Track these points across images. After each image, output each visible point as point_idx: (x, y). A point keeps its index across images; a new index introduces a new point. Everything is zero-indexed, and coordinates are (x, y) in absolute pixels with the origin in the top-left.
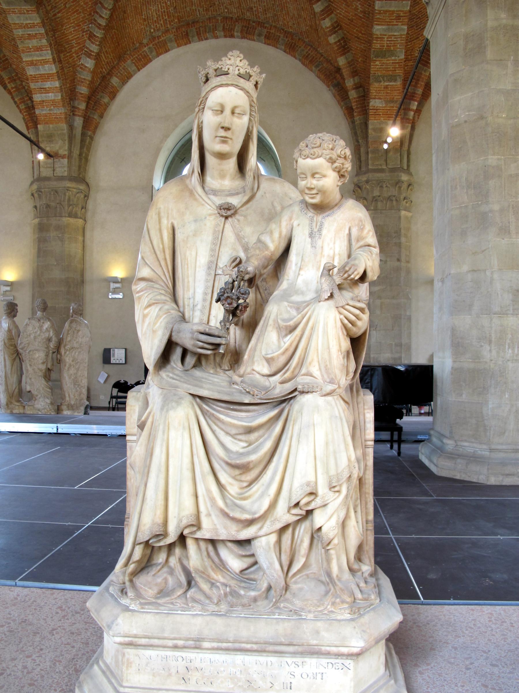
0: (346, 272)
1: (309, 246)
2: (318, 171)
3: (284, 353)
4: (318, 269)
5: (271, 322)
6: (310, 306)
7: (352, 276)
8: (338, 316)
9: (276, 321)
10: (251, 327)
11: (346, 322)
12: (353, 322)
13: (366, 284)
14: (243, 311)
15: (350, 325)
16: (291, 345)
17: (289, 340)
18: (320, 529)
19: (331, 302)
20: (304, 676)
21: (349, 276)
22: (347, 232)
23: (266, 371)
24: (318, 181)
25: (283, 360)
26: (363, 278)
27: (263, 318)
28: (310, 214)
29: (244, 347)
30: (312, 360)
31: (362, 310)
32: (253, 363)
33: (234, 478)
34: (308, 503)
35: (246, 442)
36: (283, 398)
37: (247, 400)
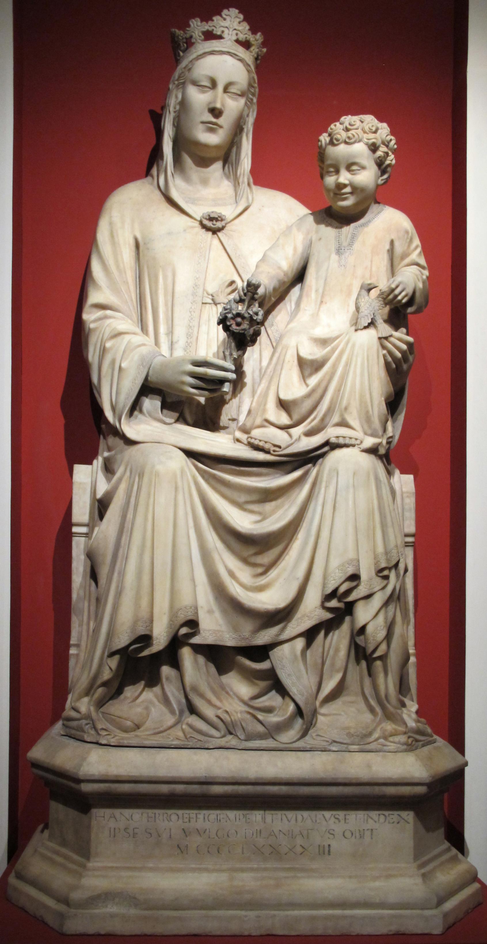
18: (363, 629)
20: (348, 834)
22: (387, 247)
25: (307, 405)
33: (245, 561)
34: (349, 592)
35: (259, 513)
37: (261, 456)
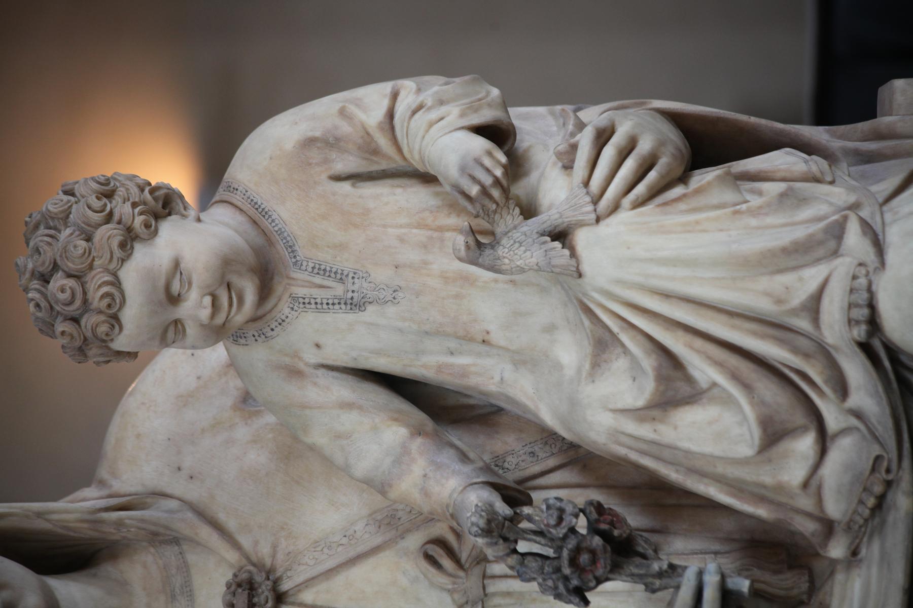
0: (485, 192)
1: (391, 310)
2: (162, 283)
3: (747, 387)
4: (467, 280)
5: (645, 431)
6: (592, 306)
7: (499, 172)
8: (625, 216)
9: (640, 414)
10: (667, 500)
11: (641, 189)
12: (640, 166)
13: (516, 122)
14: (617, 521)
15: (652, 175)
16: (719, 365)
17: (703, 369)
19: (581, 238)
21: (497, 182)
22: (346, 186)
23: (806, 444)
24: (190, 284)
25: (770, 391)
26: (498, 134)
27: (634, 456)
28: (284, 309)
29: (728, 524)
30: (767, 294)
31: (603, 137)
32: (780, 488)
36: (895, 385)
